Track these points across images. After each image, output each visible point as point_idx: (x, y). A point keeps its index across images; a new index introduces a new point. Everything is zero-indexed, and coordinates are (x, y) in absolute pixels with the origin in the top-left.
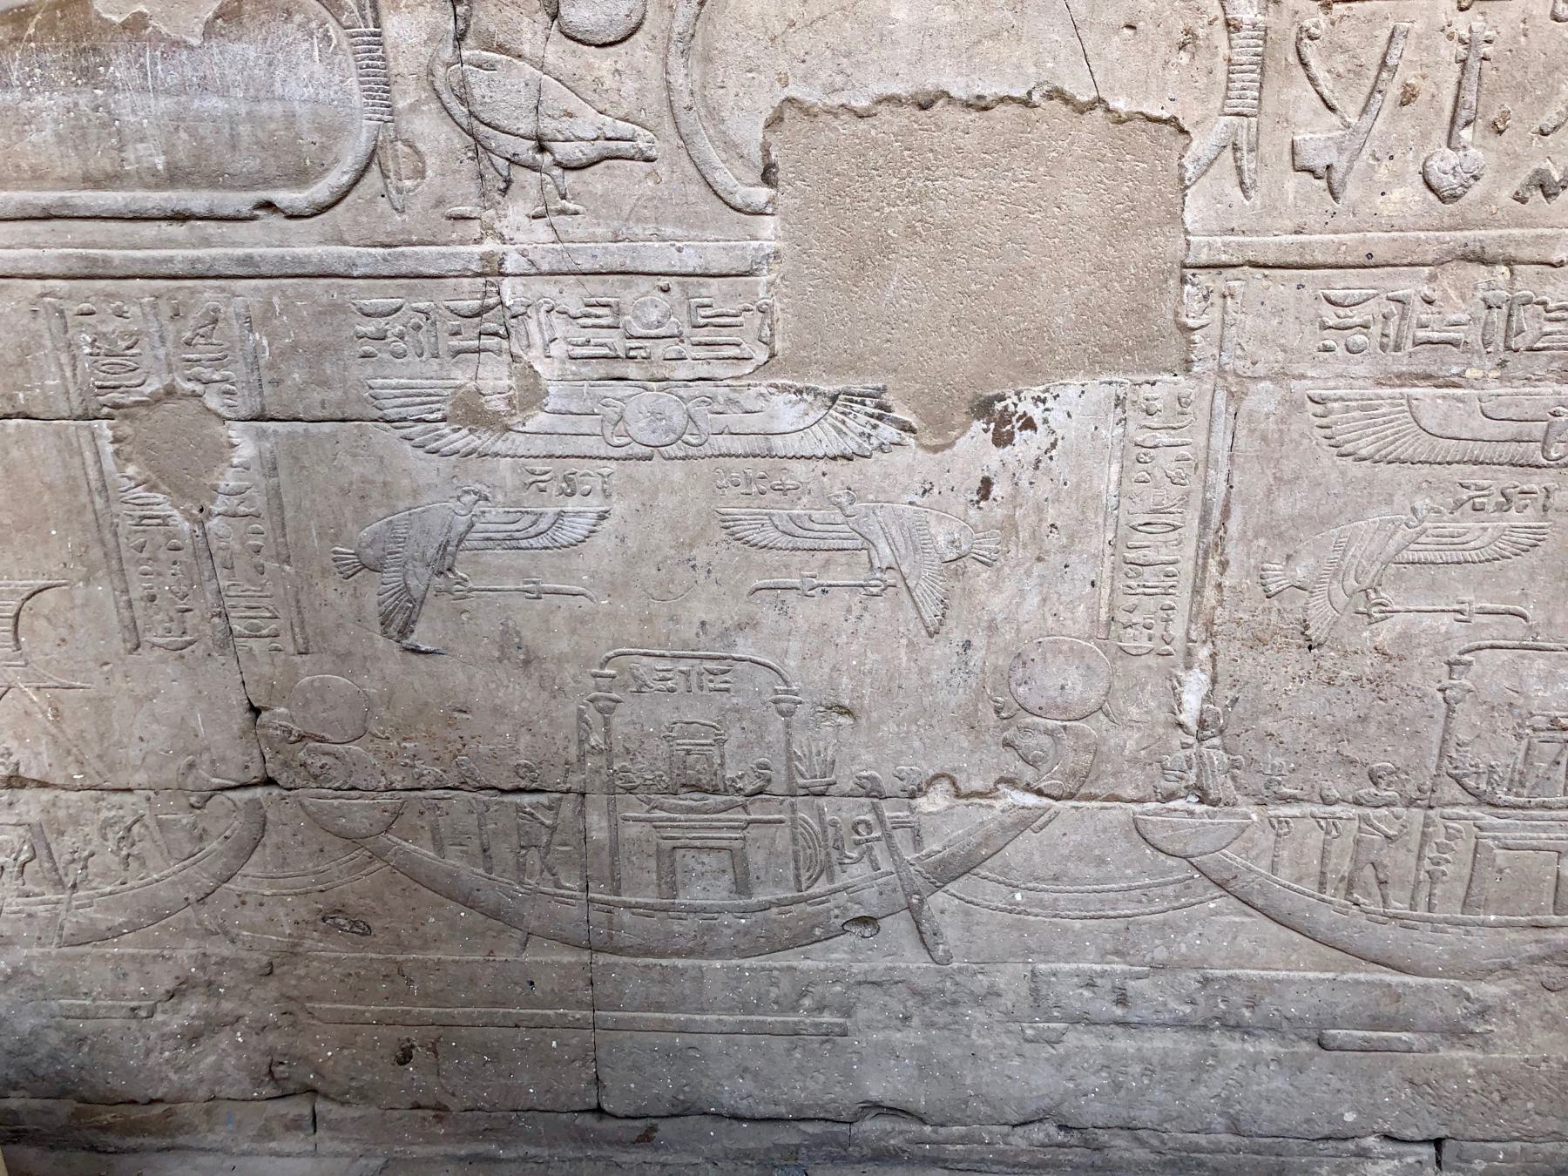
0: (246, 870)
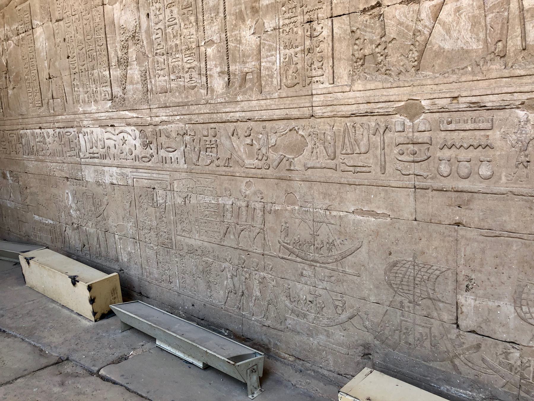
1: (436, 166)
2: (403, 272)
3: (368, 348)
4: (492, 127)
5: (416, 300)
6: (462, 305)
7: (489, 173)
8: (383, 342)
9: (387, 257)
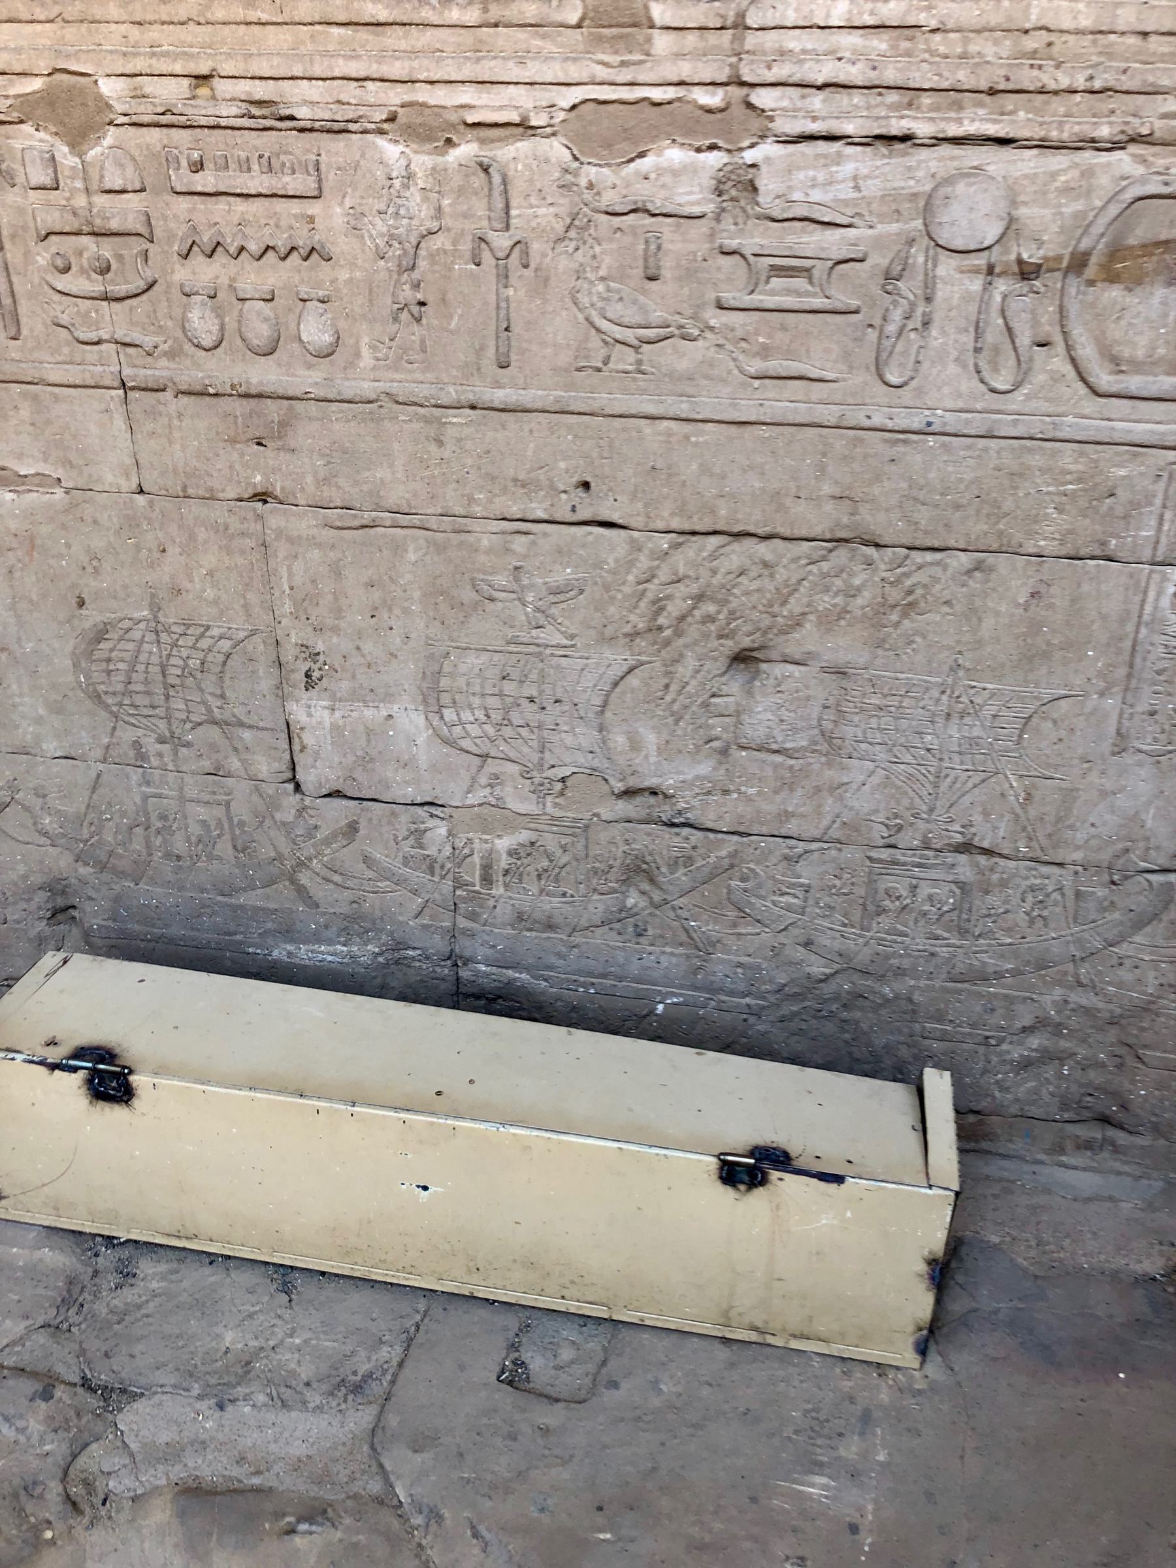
0: (1137, 939)
1: (177, 312)
2: (127, 656)
3: (63, 892)
4: (320, 189)
5: (178, 732)
6: (302, 729)
7: (327, 338)
8: (102, 867)
9: (73, 616)
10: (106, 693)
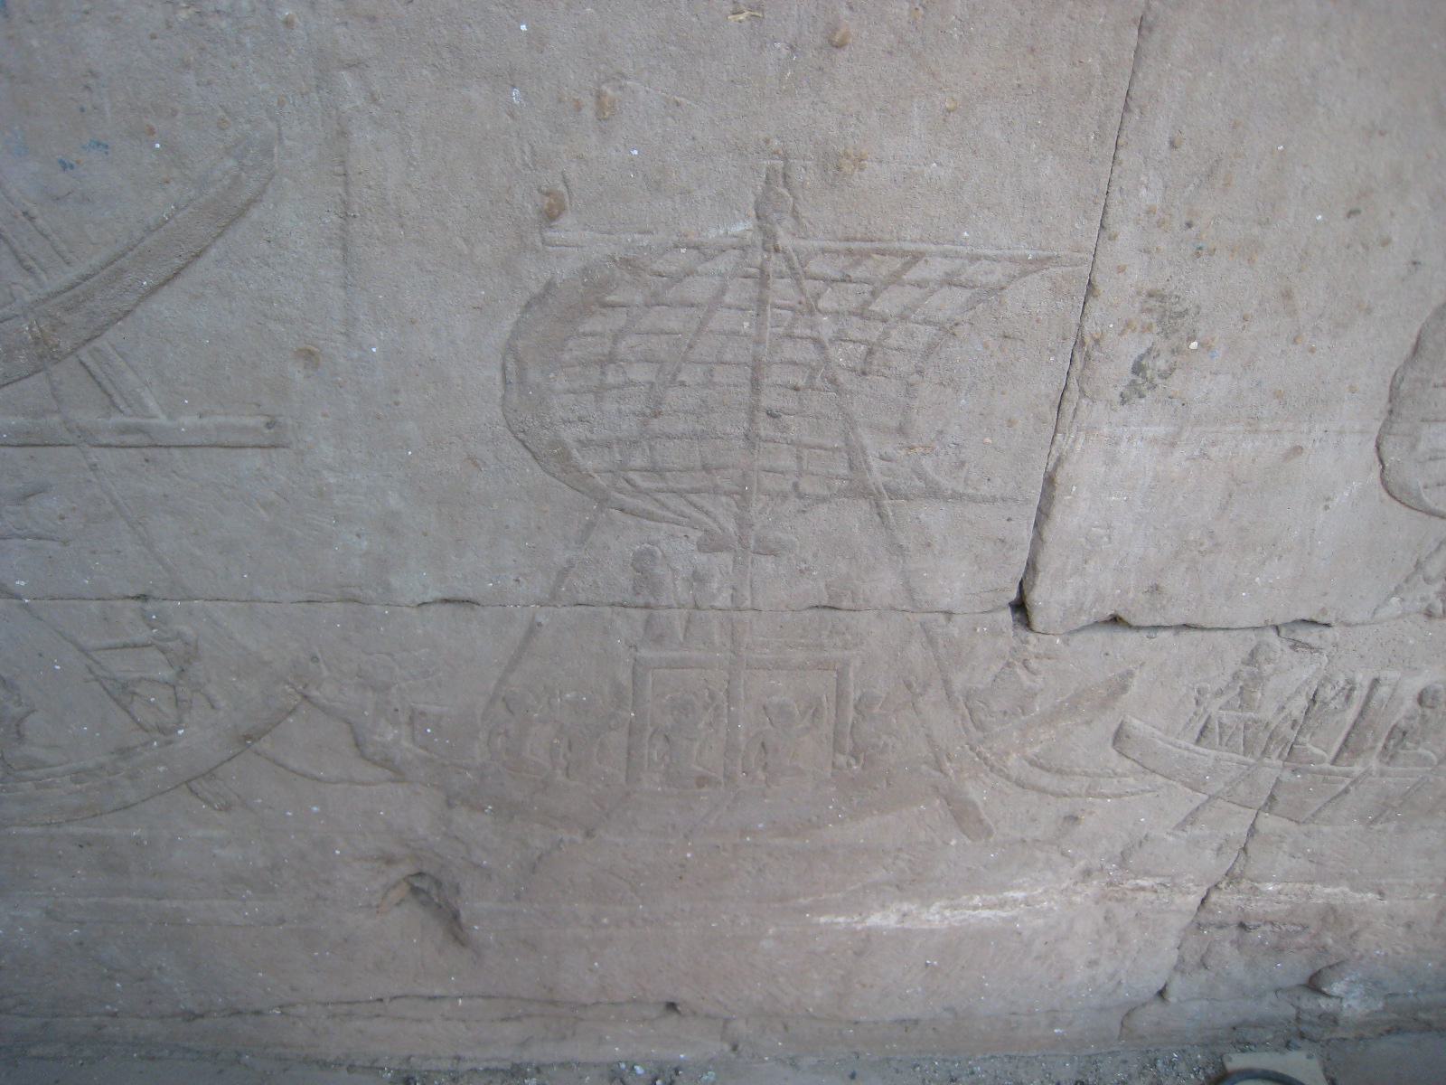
10: (584, 444)
